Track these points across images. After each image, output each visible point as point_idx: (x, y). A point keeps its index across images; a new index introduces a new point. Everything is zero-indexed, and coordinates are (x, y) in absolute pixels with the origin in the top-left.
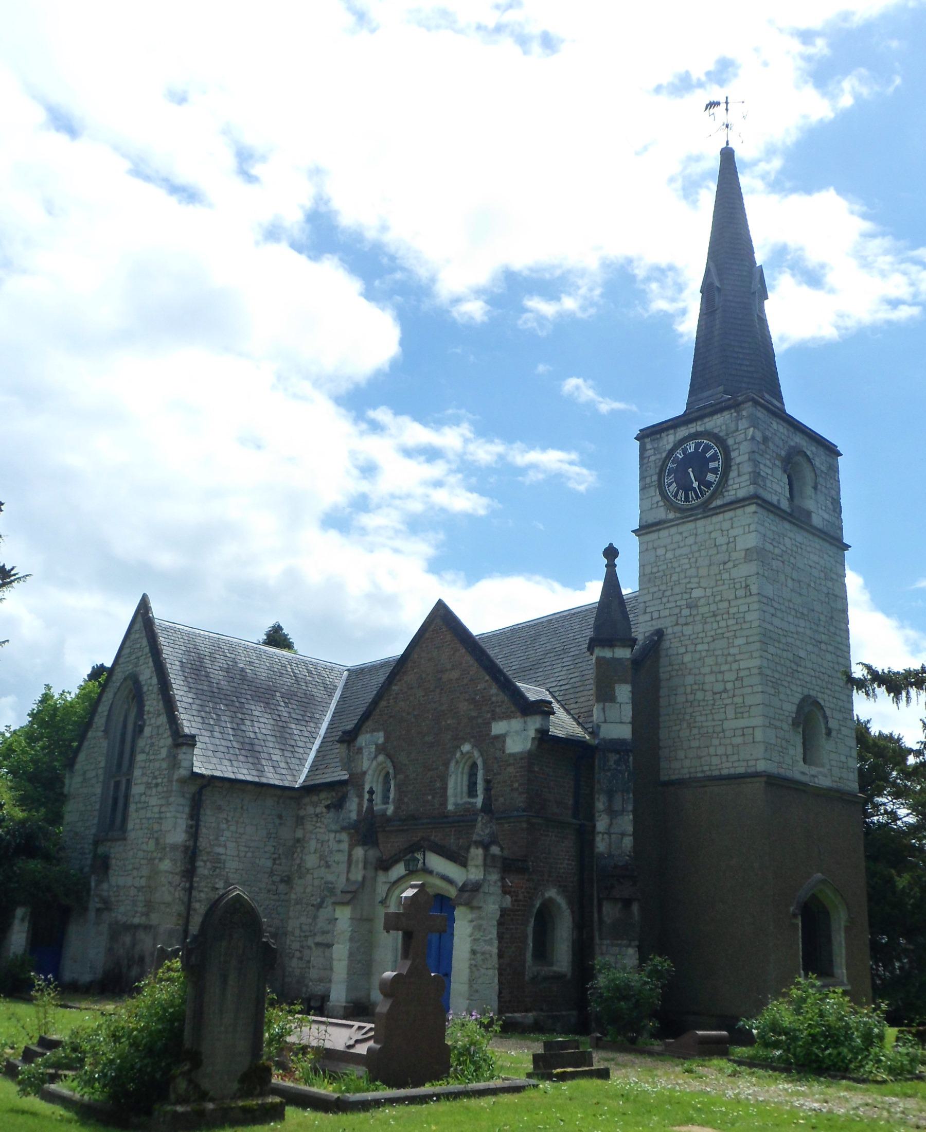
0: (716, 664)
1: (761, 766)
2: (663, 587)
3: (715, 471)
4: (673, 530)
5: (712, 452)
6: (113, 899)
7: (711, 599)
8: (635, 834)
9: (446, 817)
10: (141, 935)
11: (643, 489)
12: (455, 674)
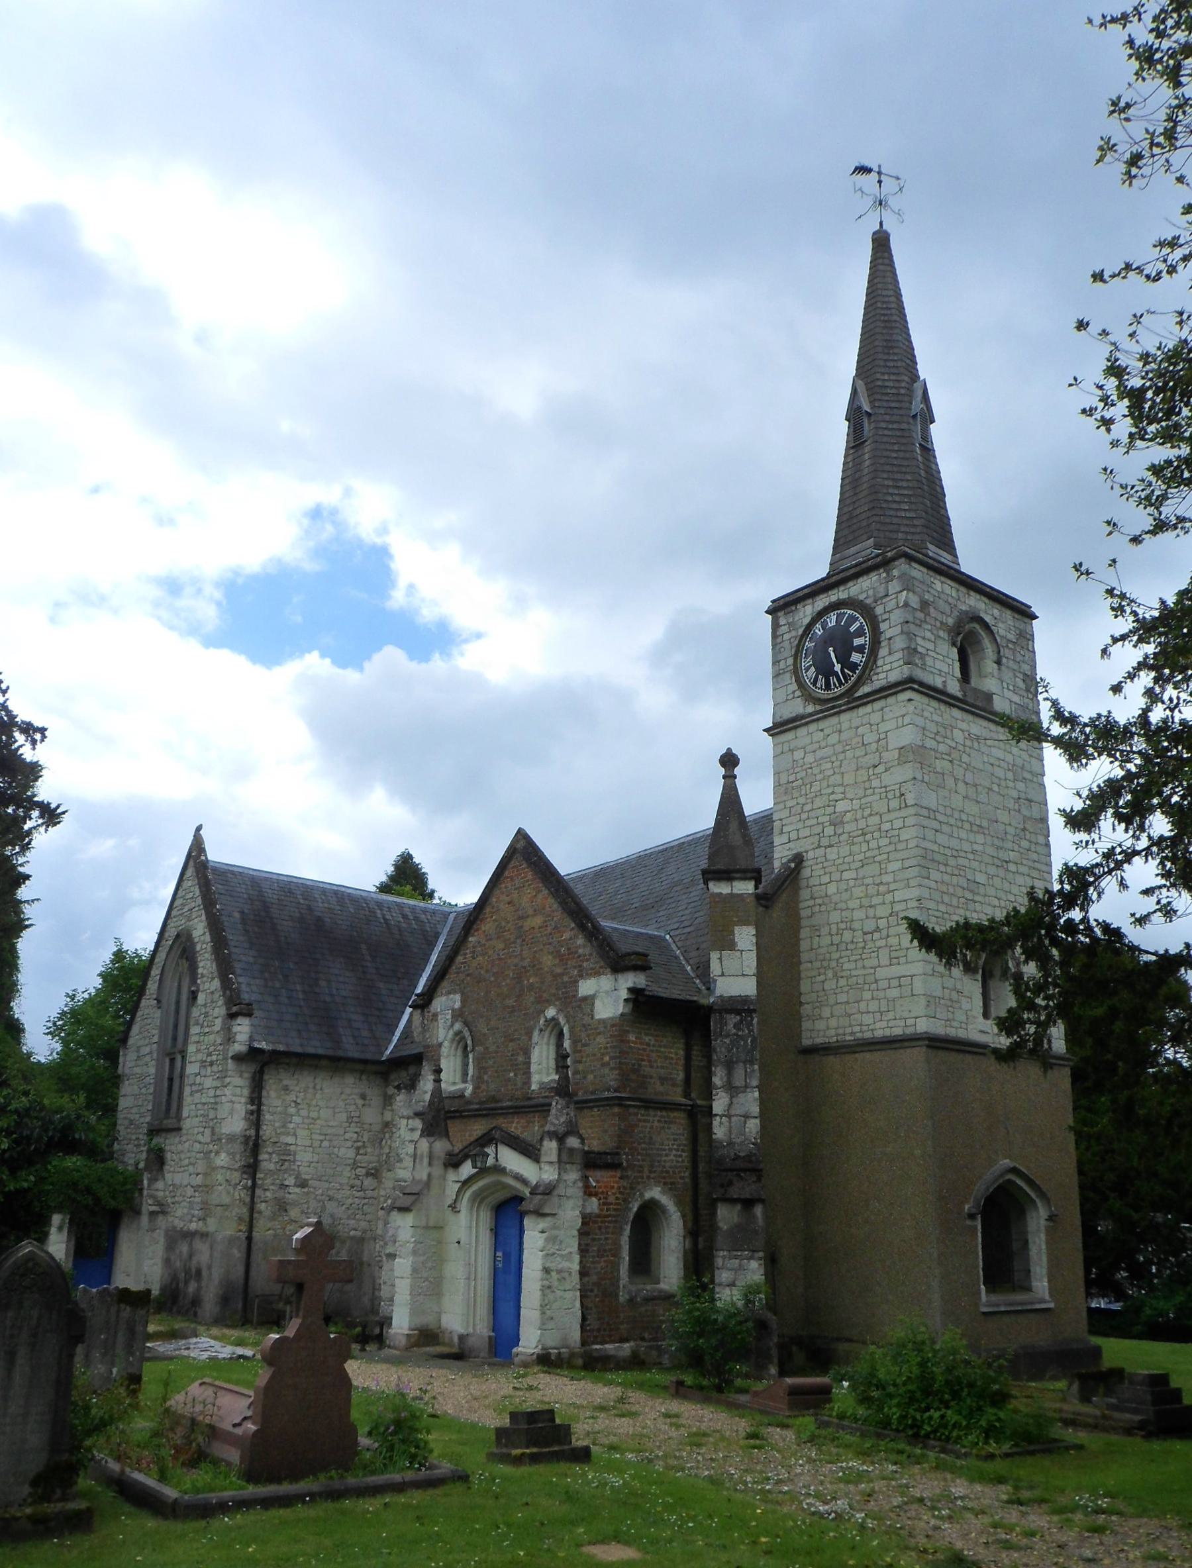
0: (866, 896)
1: (923, 1026)
2: (802, 800)
3: (860, 649)
4: (813, 727)
5: (857, 624)
6: (170, 1200)
7: (860, 812)
8: (762, 1116)
9: (530, 1099)
10: (198, 1244)
11: (776, 676)
12: (538, 921)
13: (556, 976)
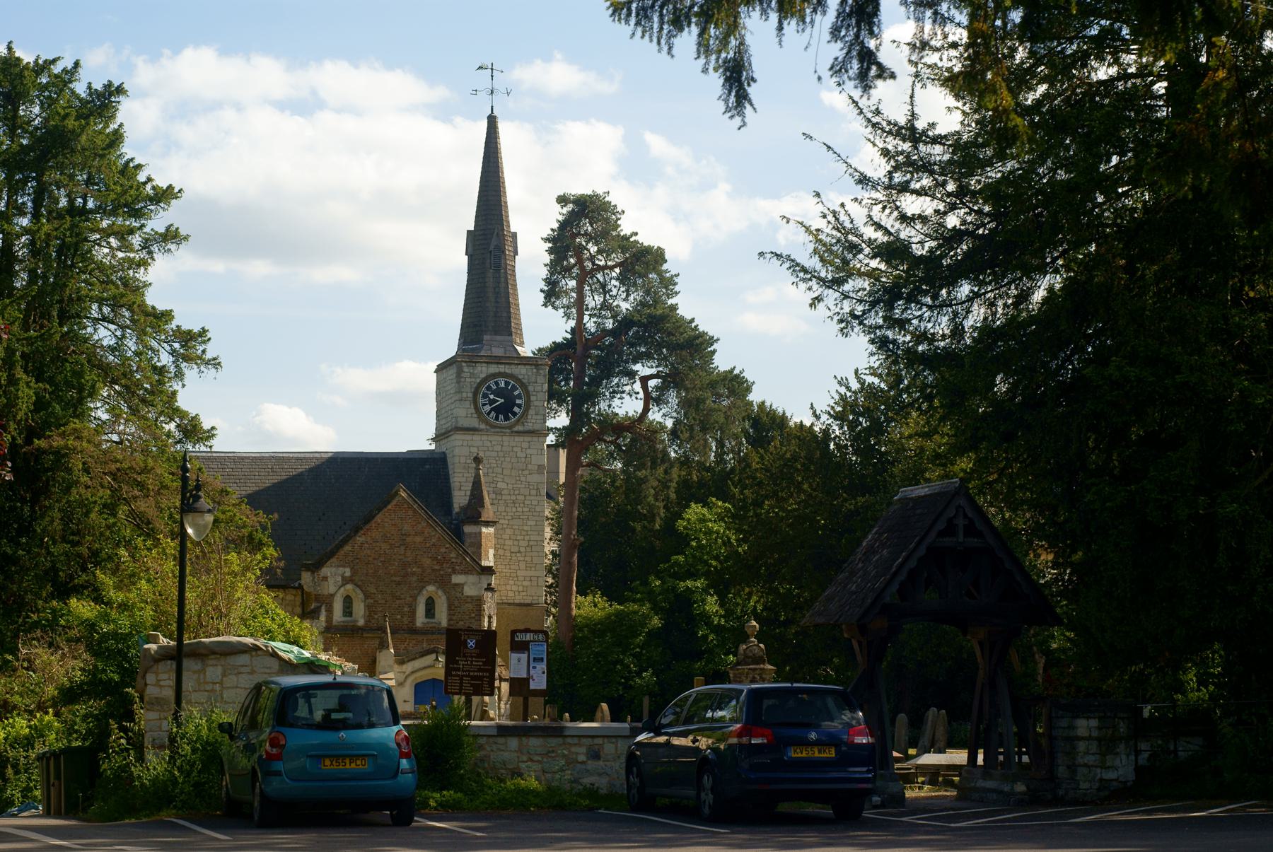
3: (519, 406)
4: (485, 438)
13: (434, 570)
